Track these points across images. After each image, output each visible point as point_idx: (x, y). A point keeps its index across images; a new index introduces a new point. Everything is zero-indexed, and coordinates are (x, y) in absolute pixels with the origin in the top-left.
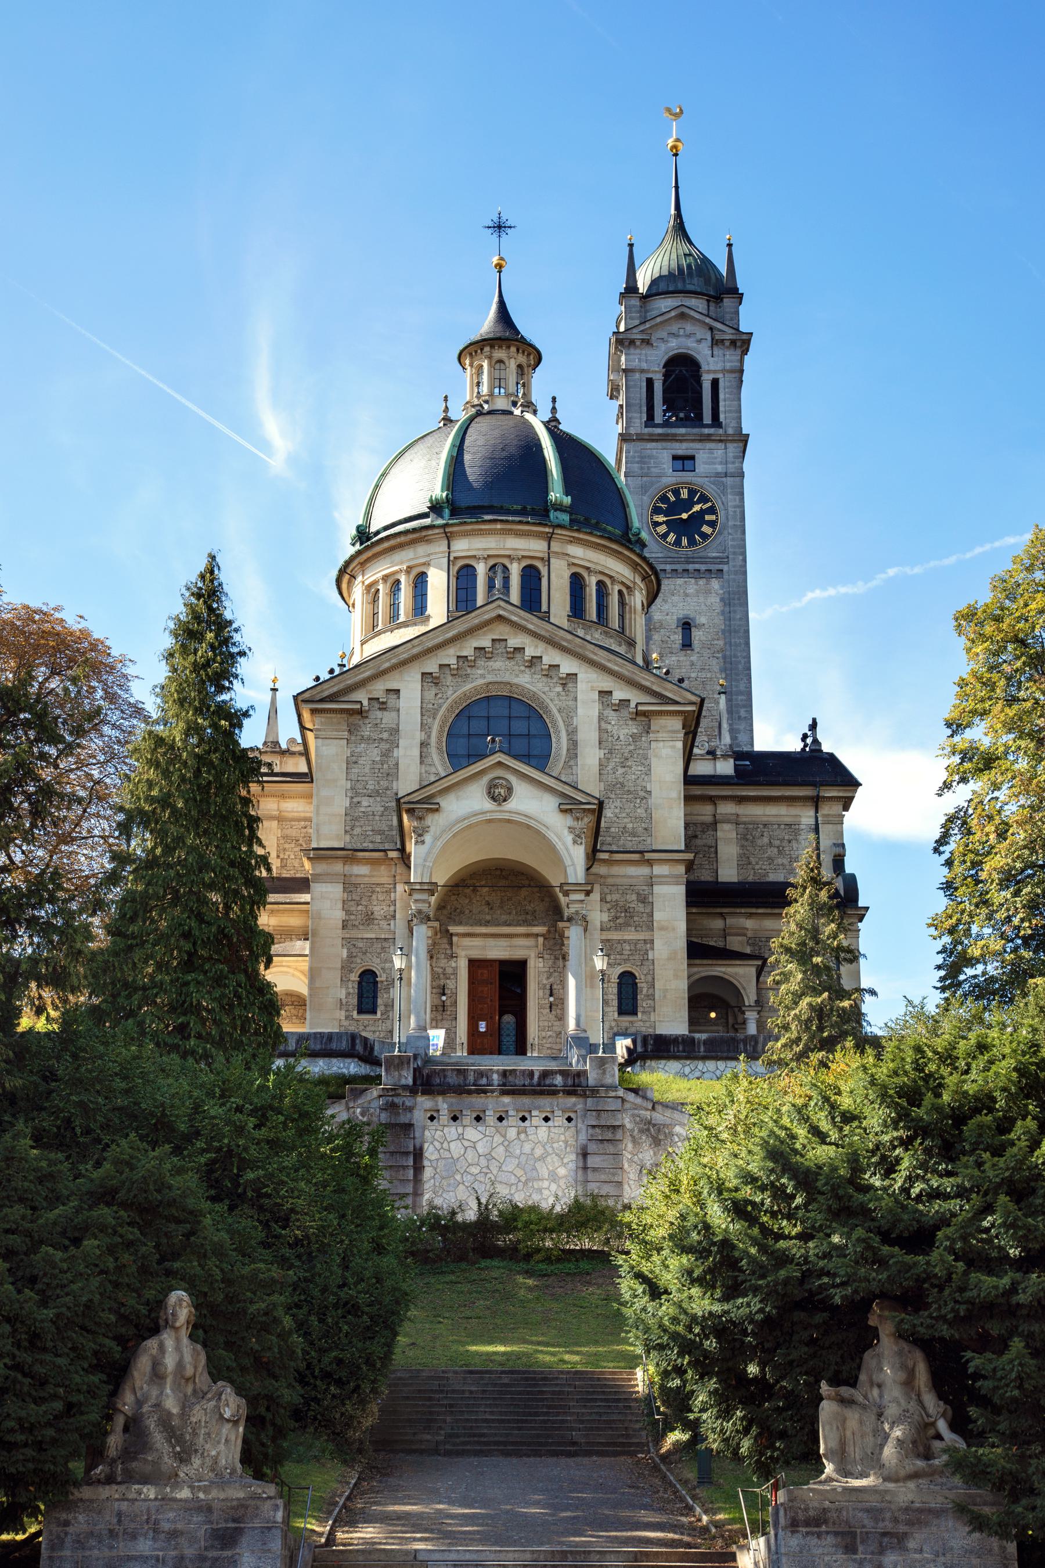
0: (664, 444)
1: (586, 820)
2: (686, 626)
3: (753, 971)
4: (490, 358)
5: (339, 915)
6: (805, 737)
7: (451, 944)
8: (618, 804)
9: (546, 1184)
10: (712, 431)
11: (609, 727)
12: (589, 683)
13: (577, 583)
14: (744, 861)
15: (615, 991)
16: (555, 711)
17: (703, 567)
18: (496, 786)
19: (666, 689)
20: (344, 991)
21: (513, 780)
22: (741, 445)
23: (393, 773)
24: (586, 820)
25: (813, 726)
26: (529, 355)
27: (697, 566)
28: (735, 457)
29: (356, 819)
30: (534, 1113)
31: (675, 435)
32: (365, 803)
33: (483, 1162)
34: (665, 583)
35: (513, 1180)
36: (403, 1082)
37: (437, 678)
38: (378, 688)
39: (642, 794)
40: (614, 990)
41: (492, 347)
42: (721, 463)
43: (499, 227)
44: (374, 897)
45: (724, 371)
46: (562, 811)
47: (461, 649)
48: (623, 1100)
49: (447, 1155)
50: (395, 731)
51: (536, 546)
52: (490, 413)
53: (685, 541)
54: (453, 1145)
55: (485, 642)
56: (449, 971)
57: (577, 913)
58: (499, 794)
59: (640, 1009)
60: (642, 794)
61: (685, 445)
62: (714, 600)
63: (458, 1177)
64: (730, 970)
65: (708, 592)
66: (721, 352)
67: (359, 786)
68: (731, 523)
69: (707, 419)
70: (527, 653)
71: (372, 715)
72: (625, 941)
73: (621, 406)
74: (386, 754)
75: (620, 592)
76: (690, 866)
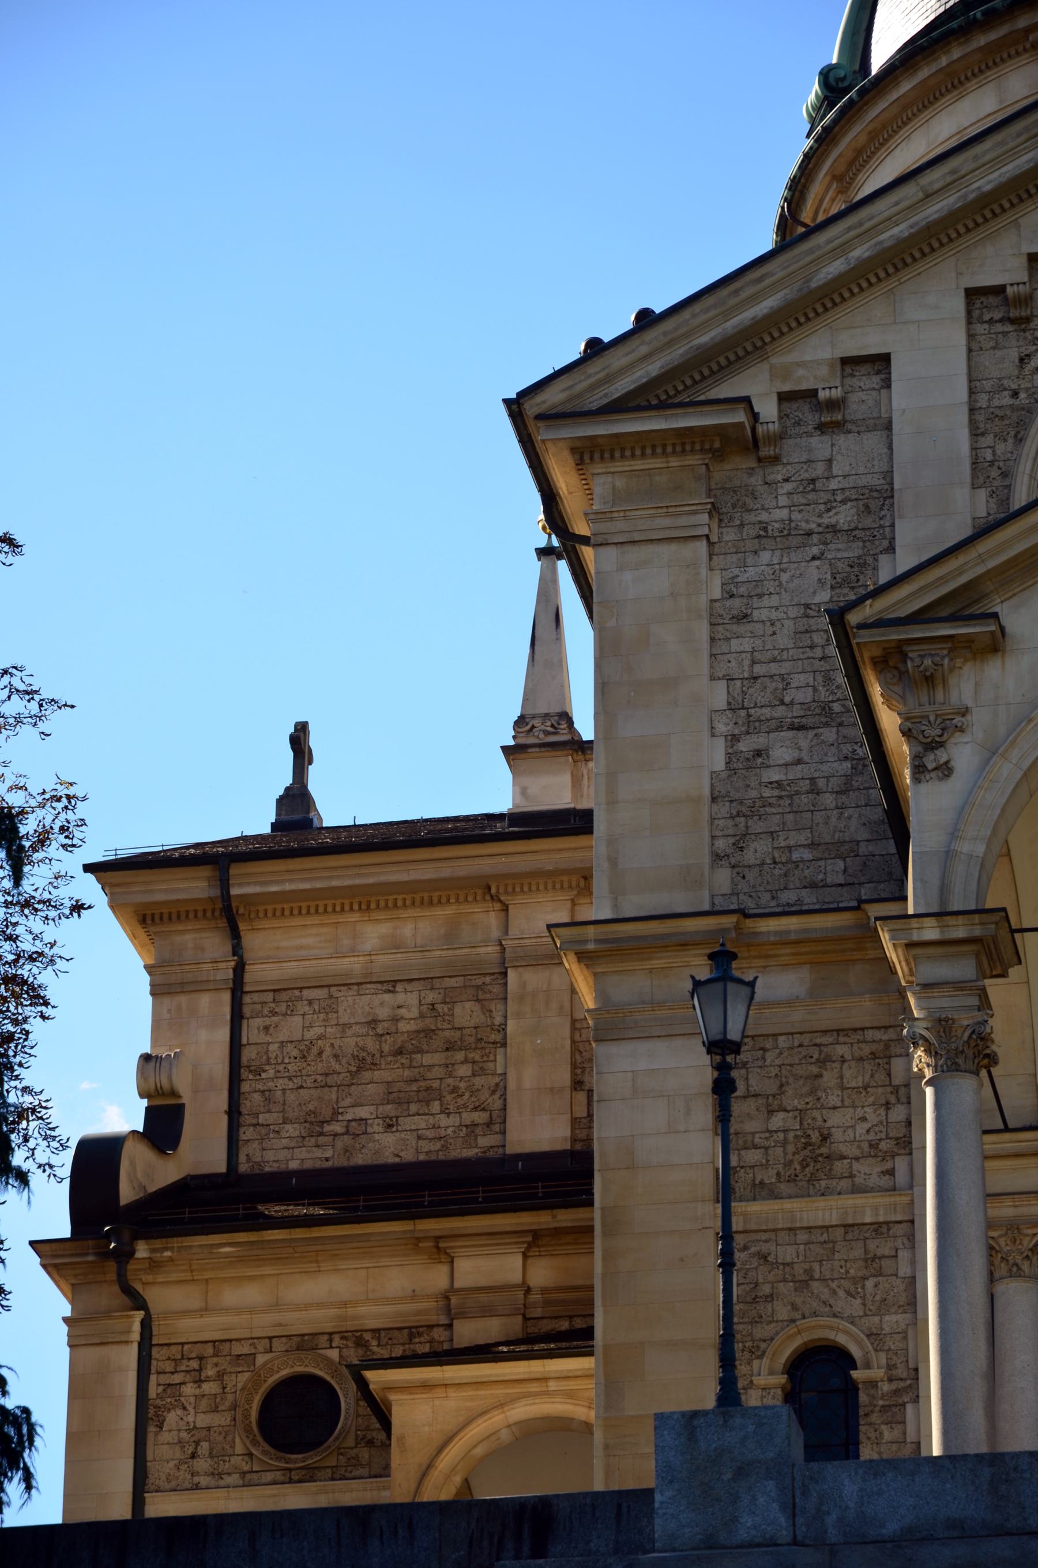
32: (781, 754)
36: (747, 1527)
38: (812, 356)
44: (829, 1078)
67: (757, 694)
71: (793, 451)
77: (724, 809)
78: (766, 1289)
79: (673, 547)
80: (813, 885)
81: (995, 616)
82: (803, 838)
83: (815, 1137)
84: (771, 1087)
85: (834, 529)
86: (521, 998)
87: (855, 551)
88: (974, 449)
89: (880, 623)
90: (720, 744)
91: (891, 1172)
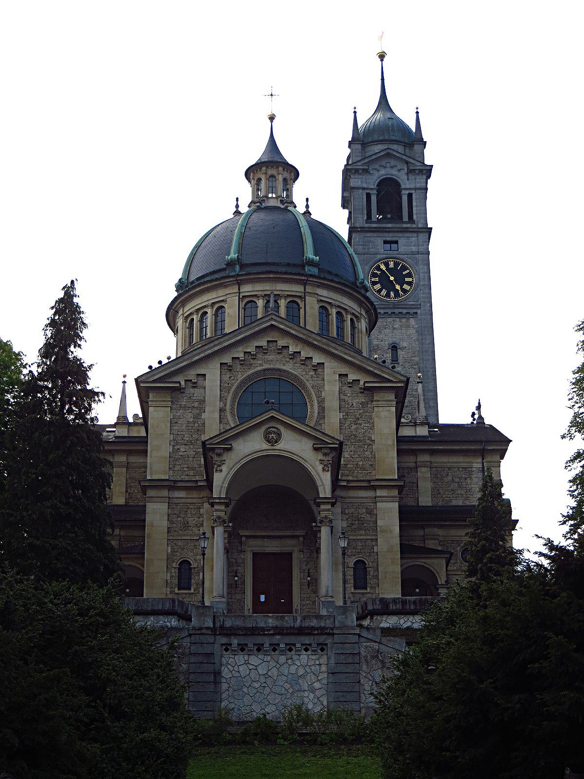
0: (378, 234)
1: (332, 455)
2: (394, 348)
3: (444, 562)
4: (266, 174)
5: (165, 523)
6: (473, 414)
7: (241, 543)
8: (352, 448)
9: (306, 694)
10: (409, 225)
11: (346, 398)
12: (331, 369)
13: (324, 310)
14: (435, 492)
15: (352, 573)
16: (310, 387)
17: (405, 311)
18: (270, 433)
19: (383, 372)
20: (169, 575)
21: (282, 429)
22: (427, 234)
23: (201, 430)
24: (332, 455)
25: (479, 408)
26: (291, 172)
27: (400, 310)
28: (423, 242)
29: (176, 460)
30: (298, 645)
31: (386, 228)
32: (182, 450)
33: (263, 680)
34: (380, 320)
35: (283, 691)
36: (206, 625)
37: (230, 366)
38: (192, 374)
39: (368, 442)
40: (350, 572)
41: (267, 167)
42: (414, 245)
43: (272, 95)
45: (415, 189)
46: (316, 449)
47: (247, 347)
48: (359, 635)
49: (237, 675)
50: (202, 401)
51: (297, 289)
52: (266, 208)
53: (392, 294)
54: (241, 669)
55: (263, 343)
56: (240, 561)
57: (326, 517)
58: (273, 438)
59: (369, 585)
60: (368, 442)
61: (391, 234)
62: (412, 331)
63: (245, 690)
64: (428, 561)
65: (408, 327)
66: (413, 177)
68: (422, 283)
69: (405, 218)
70: (291, 349)
71: (187, 391)
72: (358, 540)
73: (350, 213)
74: (197, 417)
75: (352, 320)
76: (400, 489)
77: (172, 459)
78: (176, 550)
79: (164, 408)
80: (188, 475)
81: (231, 444)
82: (186, 466)
83: (186, 522)
84: (178, 513)
85: (194, 407)
86: (116, 474)
87: (197, 412)
88: (220, 394)
89: (212, 444)
90: (171, 446)
91: (199, 530)
